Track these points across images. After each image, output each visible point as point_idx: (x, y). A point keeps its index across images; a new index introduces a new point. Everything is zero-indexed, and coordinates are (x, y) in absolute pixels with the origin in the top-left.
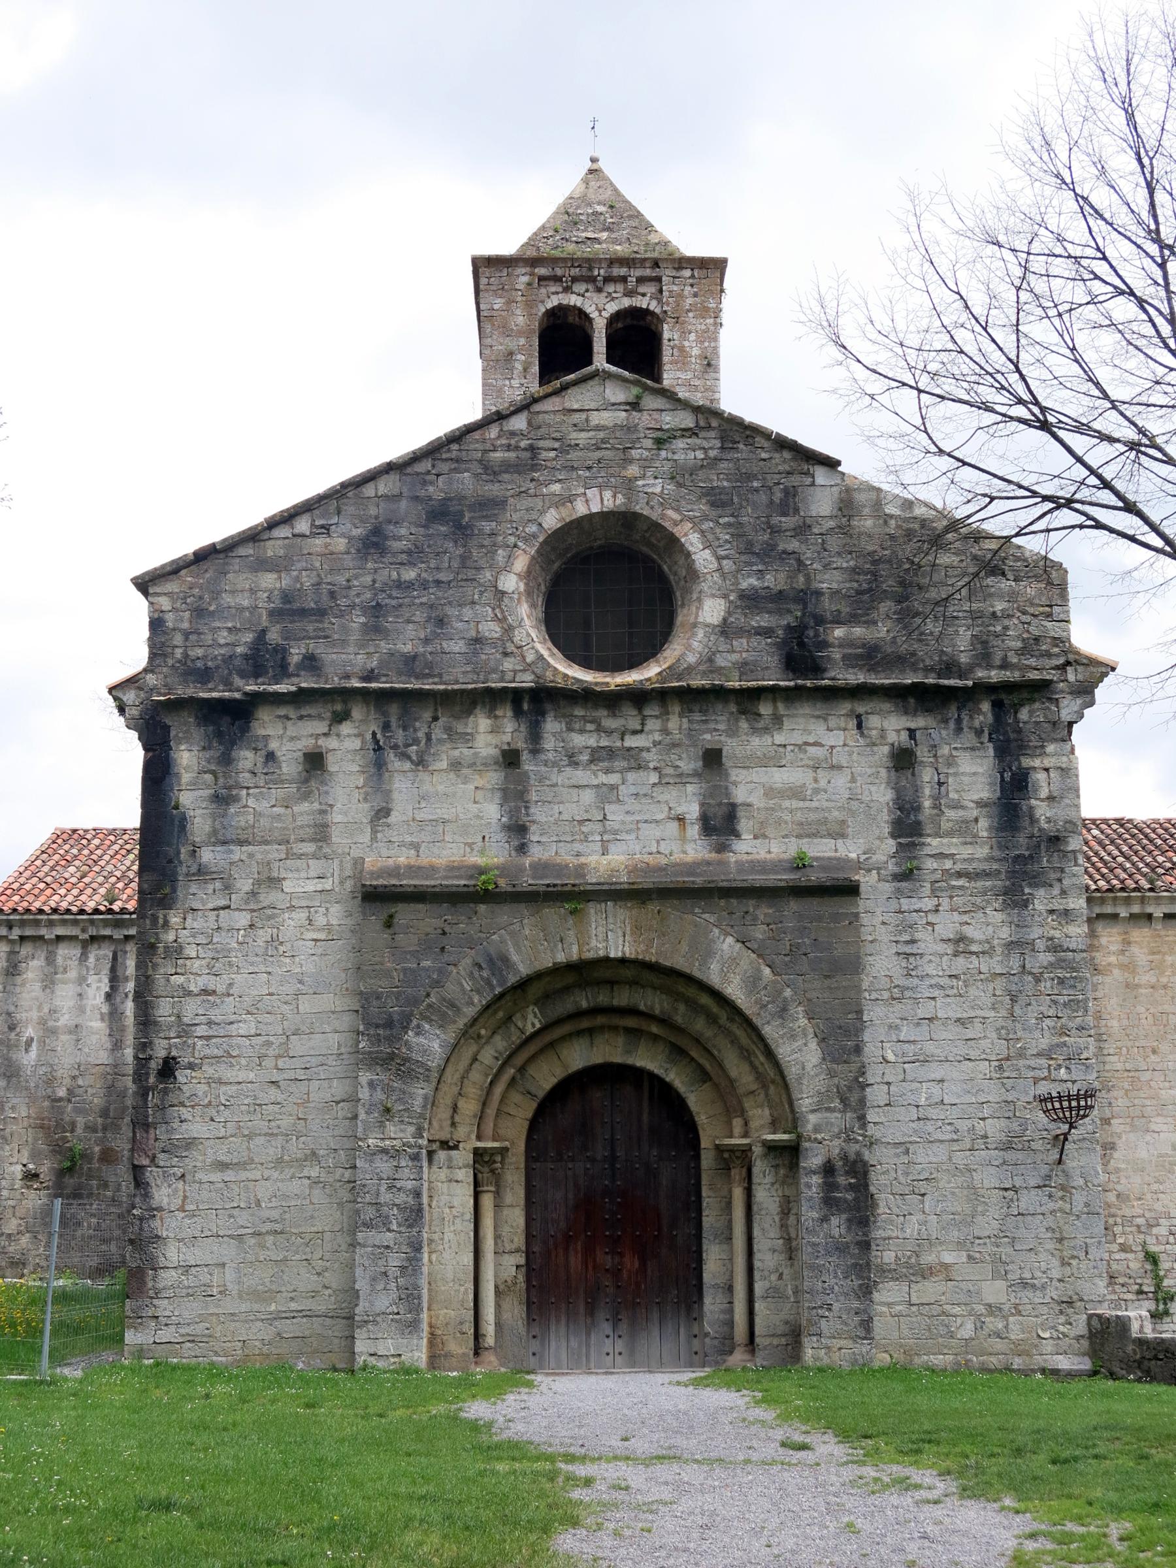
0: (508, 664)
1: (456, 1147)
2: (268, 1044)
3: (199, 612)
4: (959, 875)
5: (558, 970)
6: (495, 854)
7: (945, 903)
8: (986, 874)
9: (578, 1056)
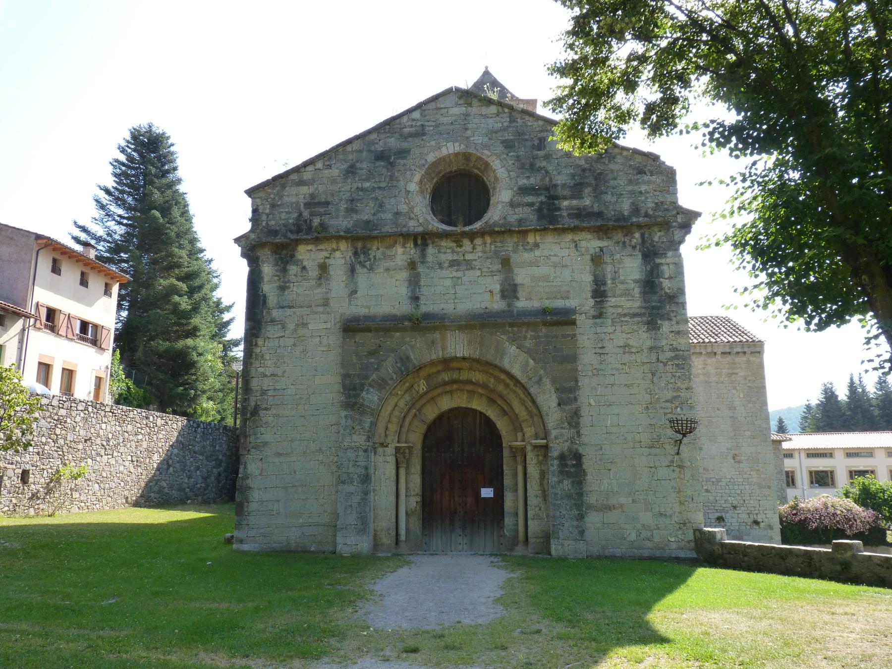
0: (412, 223)
1: (387, 446)
2: (301, 398)
3: (273, 206)
4: (625, 315)
5: (433, 363)
6: (405, 308)
7: (619, 329)
9: (446, 404)
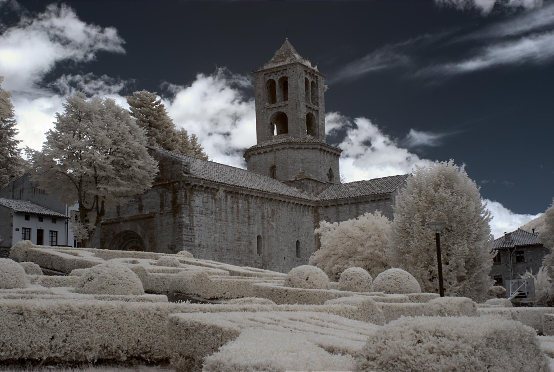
8: (170, 212)
